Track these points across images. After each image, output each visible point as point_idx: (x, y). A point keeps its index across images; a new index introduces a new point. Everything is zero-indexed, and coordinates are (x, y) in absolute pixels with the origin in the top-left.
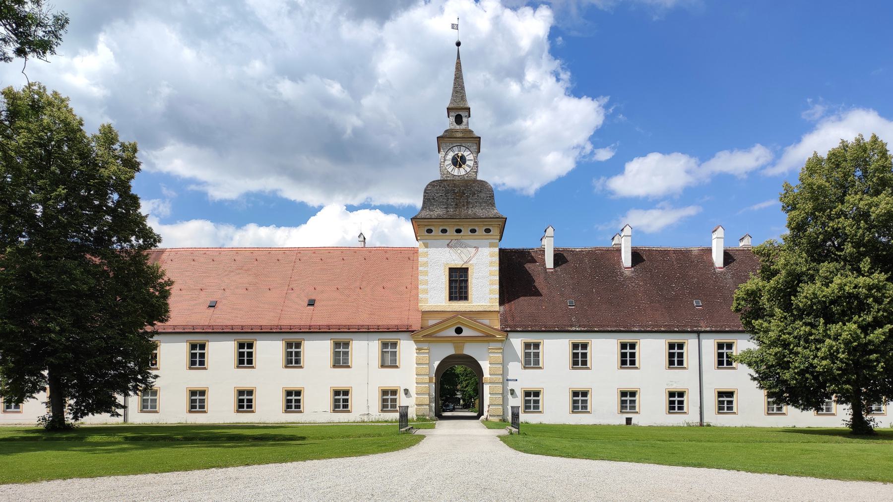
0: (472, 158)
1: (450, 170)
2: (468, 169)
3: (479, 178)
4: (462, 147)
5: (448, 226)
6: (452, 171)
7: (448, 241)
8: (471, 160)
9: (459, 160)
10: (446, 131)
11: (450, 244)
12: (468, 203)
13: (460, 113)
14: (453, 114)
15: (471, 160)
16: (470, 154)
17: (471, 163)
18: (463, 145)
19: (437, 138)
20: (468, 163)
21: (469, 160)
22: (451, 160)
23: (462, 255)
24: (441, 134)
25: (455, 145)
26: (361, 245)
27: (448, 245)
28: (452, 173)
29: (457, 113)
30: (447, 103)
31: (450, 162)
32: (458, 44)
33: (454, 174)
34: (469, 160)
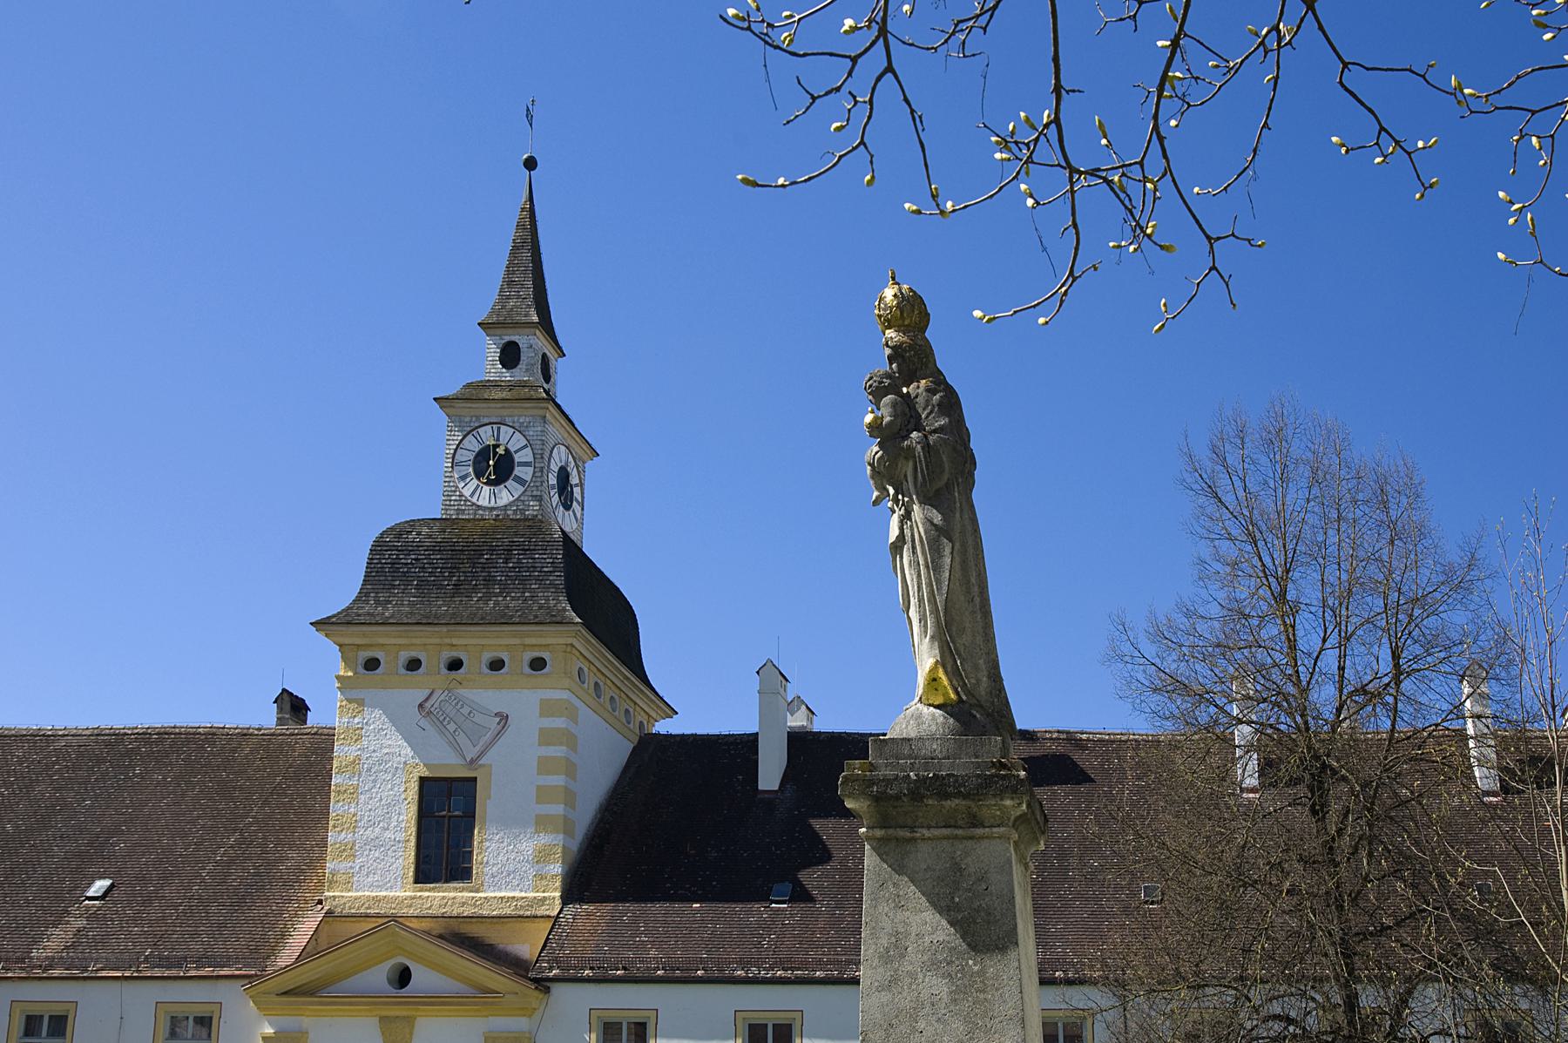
0: (530, 459)
2: (518, 490)
6: (472, 495)
7: (421, 695)
8: (526, 464)
10: (468, 386)
11: (428, 705)
12: (489, 581)
13: (515, 338)
15: (526, 464)
16: (526, 446)
18: (508, 420)
20: (518, 471)
21: (521, 464)
22: (471, 463)
23: (462, 738)
25: (486, 420)
26: (265, 717)
27: (421, 706)
28: (474, 500)
29: (507, 339)
32: (531, 164)
33: (480, 503)
34: (521, 464)
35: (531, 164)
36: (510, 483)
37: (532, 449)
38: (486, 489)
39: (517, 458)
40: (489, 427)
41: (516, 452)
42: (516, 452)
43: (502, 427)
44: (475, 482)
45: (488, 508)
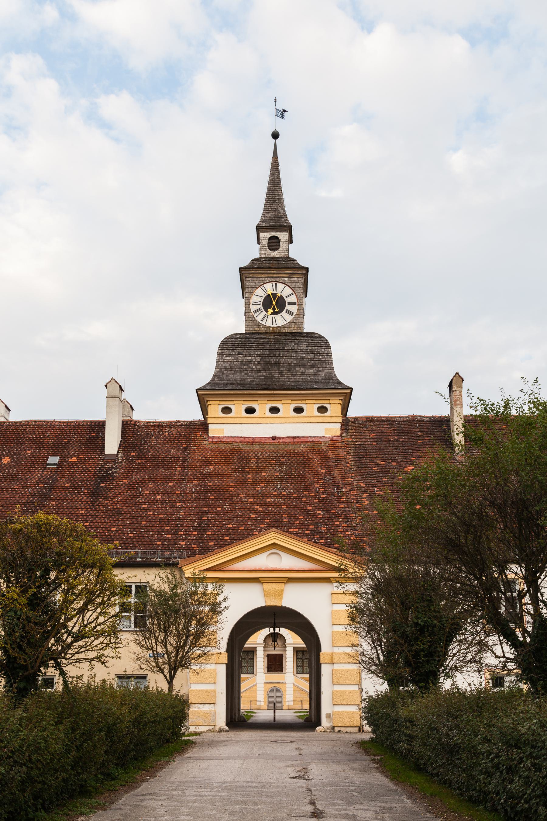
1: (259, 319)
3: (307, 328)
4: (278, 284)
5: (256, 402)
6: (262, 320)
8: (294, 304)
9: (274, 303)
14: (265, 236)
15: (294, 304)
16: (292, 294)
17: (294, 309)
19: (240, 268)
20: (288, 307)
21: (290, 304)
22: (261, 303)
24: (246, 263)
28: (263, 323)
30: (257, 217)
31: (261, 306)
34: (290, 304)
35: (275, 136)
36: (284, 313)
37: (296, 295)
38: (270, 317)
39: (287, 300)
40: (271, 283)
41: (287, 297)
42: (287, 297)
43: (278, 283)
44: (264, 313)
45: (272, 327)
